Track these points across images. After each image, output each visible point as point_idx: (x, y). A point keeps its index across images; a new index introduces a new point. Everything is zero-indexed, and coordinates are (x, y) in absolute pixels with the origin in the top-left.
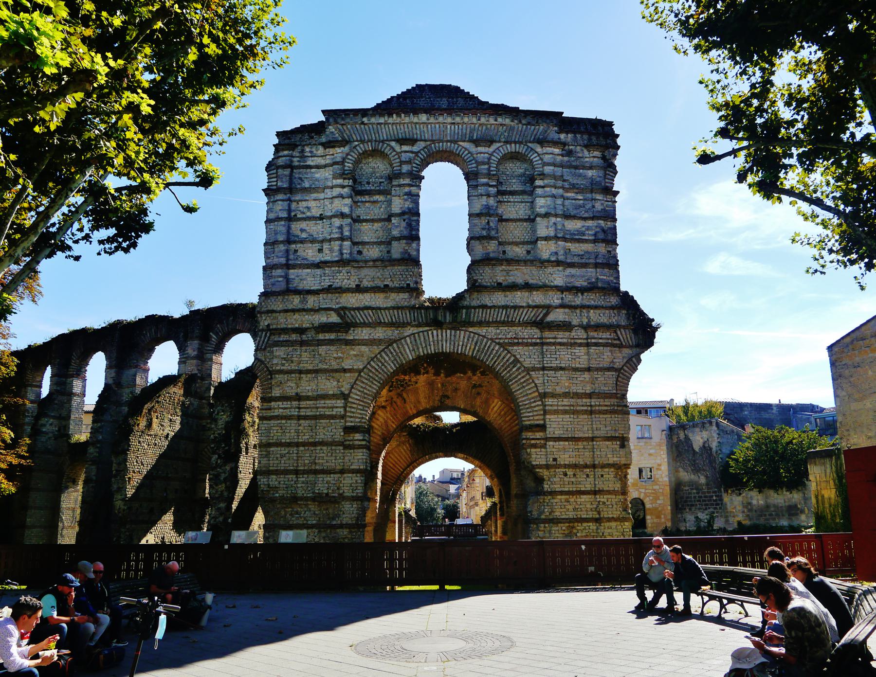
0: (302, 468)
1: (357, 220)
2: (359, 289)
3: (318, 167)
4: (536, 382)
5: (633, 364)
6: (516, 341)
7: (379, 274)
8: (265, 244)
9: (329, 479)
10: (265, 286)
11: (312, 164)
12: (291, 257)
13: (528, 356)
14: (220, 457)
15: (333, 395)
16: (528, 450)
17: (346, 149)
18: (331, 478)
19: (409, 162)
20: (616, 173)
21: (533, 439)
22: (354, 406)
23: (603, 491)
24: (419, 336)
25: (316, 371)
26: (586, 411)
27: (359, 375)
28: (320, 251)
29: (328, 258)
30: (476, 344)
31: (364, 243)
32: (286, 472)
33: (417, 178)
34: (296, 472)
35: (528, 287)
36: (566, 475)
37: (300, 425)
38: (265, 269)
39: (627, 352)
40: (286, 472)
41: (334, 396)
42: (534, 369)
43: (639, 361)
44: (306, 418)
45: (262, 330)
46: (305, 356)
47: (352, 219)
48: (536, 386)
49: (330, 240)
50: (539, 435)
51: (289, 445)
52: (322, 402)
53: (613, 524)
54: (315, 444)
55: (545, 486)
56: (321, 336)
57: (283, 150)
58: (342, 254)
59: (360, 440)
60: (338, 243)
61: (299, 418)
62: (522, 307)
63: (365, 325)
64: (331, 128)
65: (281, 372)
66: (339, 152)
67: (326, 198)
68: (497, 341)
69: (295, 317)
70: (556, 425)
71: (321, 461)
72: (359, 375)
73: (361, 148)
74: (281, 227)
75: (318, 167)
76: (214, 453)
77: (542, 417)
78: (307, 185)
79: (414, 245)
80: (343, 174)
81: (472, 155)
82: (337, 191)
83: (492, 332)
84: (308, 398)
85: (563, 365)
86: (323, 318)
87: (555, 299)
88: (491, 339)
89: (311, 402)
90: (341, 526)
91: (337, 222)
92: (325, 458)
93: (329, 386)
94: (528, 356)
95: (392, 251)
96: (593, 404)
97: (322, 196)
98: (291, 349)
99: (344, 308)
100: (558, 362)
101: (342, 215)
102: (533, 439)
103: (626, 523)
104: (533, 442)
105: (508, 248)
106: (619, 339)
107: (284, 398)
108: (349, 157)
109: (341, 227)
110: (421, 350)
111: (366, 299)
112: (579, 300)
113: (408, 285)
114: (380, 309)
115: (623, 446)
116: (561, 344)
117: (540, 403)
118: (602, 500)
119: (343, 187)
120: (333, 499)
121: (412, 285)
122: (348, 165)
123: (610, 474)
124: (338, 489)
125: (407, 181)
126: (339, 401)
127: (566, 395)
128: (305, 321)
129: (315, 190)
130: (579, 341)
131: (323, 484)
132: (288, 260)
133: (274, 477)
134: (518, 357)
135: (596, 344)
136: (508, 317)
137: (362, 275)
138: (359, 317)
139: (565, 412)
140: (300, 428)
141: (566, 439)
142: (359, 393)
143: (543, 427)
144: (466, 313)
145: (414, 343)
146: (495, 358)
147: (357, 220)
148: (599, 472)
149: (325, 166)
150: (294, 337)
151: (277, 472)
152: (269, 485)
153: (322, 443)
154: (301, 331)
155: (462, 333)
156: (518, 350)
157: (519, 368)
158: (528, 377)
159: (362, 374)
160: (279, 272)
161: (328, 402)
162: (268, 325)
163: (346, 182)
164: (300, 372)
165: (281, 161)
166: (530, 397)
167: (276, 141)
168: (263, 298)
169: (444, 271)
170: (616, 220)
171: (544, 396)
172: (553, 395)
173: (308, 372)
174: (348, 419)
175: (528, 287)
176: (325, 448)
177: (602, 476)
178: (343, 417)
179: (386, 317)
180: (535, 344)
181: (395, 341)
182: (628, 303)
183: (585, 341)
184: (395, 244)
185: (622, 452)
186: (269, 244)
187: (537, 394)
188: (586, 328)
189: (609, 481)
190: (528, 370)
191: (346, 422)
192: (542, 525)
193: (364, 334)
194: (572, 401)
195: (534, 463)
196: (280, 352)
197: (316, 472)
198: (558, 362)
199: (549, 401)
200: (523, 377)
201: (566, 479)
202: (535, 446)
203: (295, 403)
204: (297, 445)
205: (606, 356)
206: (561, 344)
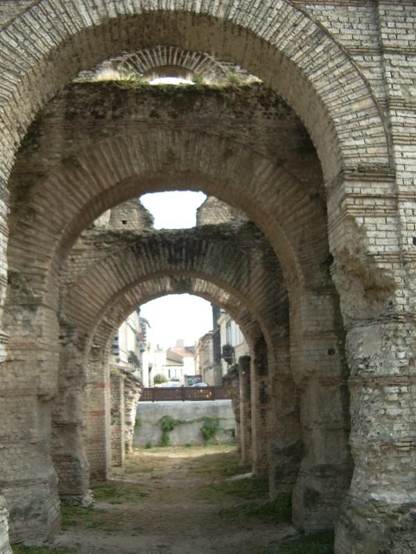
4: (367, 75)
16: (360, 220)
21: (369, 197)
48: (368, 85)
50: (378, 188)
55: (400, 300)
104: (367, 202)
134: (325, 24)
143: (387, 173)
166: (356, 107)
190: (347, 54)
192: (394, 390)
195: (372, 250)
200: (338, 66)
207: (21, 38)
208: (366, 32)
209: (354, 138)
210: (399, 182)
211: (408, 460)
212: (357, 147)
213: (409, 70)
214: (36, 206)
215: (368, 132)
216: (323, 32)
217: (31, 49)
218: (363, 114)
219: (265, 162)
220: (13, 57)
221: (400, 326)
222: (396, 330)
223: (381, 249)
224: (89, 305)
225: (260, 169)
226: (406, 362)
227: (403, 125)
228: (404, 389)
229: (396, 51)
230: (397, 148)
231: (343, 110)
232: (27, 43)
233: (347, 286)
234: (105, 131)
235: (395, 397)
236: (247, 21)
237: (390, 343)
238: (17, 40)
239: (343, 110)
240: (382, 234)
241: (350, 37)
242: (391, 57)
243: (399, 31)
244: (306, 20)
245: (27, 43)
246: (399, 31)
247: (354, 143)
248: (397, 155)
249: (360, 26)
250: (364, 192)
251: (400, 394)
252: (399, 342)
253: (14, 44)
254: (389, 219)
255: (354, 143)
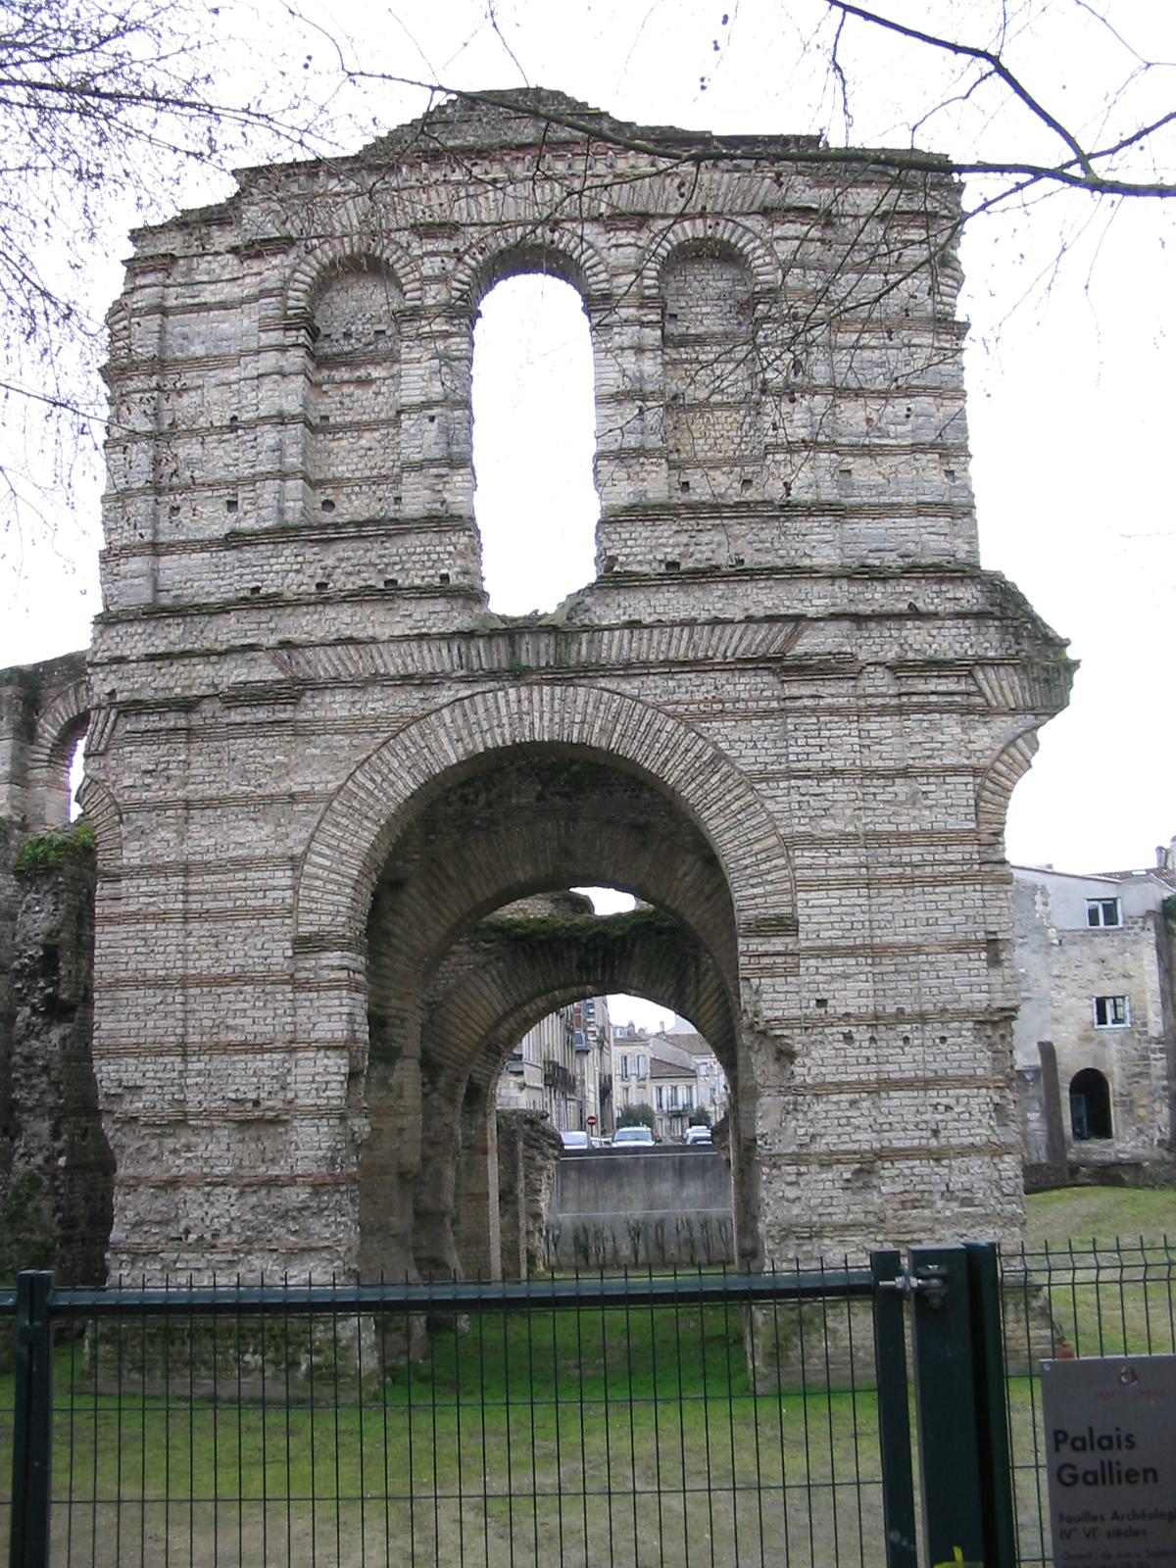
0: (196, 1039)
1: (319, 427)
2: (323, 596)
3: (223, 305)
4: (770, 805)
5: (1017, 754)
6: (717, 707)
7: (372, 556)
8: (104, 499)
9: (261, 1065)
10: (107, 598)
11: (212, 299)
12: (164, 524)
13: (747, 745)
14: (35, 1011)
15: (267, 858)
17: (290, 259)
18: (263, 1063)
19: (443, 278)
20: (960, 282)
21: (766, 954)
22: (318, 883)
23: (946, 1078)
24: (473, 705)
25: (221, 802)
26: (901, 876)
27: (329, 808)
28: (232, 505)
29: (249, 524)
30: (616, 718)
31: (338, 483)
32: (160, 1051)
33: (464, 312)
34: (184, 1050)
35: (743, 573)
36: (848, 1038)
37: (189, 935)
38: (105, 557)
39: (1005, 726)
40: (160, 1051)
41: (268, 861)
42: (766, 777)
43: (1034, 746)
44: (205, 916)
45: (99, 707)
46: (200, 765)
47: (307, 424)
49: (253, 480)
50: (778, 944)
51: (161, 984)
52: (241, 875)
53: (975, 1163)
54: (221, 981)
56: (235, 717)
57: (144, 273)
58: (281, 512)
59: (333, 968)
60: (273, 485)
61: (186, 917)
62: (731, 622)
63: (336, 683)
64: (251, 213)
65: (142, 806)
66: (272, 270)
67: (243, 374)
68: (669, 708)
69: (173, 669)
70: (823, 914)
71: (238, 1021)
72: (329, 808)
73: (326, 253)
74: (141, 456)
75: (223, 305)
76: (23, 1001)
77: (786, 898)
78: (198, 350)
79: (458, 478)
80: (285, 317)
81: (597, 253)
82: (269, 361)
83: (653, 688)
84: (207, 868)
85: (839, 764)
86: (235, 673)
87: (815, 599)
88: (658, 708)
89: (213, 878)
90: (292, 1181)
91: (269, 436)
92: (253, 1015)
93: (253, 836)
94: (747, 745)
95: (406, 497)
96: (916, 858)
97: (232, 375)
98: (164, 749)
99: (286, 645)
100: (826, 756)
101: (281, 419)
102: (766, 954)
103: (1006, 1158)
104: (765, 961)
105: (694, 477)
106: (981, 693)
107: (158, 870)
108: (297, 275)
109: (279, 448)
110: (478, 738)
111: (343, 620)
112: (878, 597)
113: (445, 578)
114: (374, 640)
115: (995, 962)
116: (832, 711)
117: (782, 861)
118: (945, 1101)
119: (283, 349)
120: (270, 1114)
121: (453, 580)
122: (297, 299)
123: (964, 1036)
124: (283, 1088)
125: (439, 325)
126: (280, 874)
127: (846, 839)
128: (201, 676)
129: (220, 361)
130: (879, 701)
131: (246, 1077)
132: (156, 533)
133: (132, 1061)
134: (723, 746)
135: (922, 708)
136: (695, 648)
137: (330, 562)
138: (324, 664)
139: (848, 883)
140: (191, 940)
141: (851, 952)
142: (328, 852)
143: (786, 925)
144: (590, 642)
145: (460, 721)
146: (664, 753)
147: (319, 427)
148: (934, 1031)
149: (243, 301)
150: (173, 720)
151: (137, 1051)
152: (120, 1080)
153: (240, 978)
154: (187, 705)
155: (581, 691)
156: (723, 731)
157: (728, 775)
158: (749, 798)
159: (335, 804)
160: (137, 564)
161: (251, 875)
162: (112, 694)
163: (292, 337)
164: (188, 805)
165: (141, 299)
166: (757, 847)
167: (129, 251)
168: (100, 627)
169: (537, 542)
170: (964, 394)
171: (789, 843)
172: (813, 841)
173: (207, 803)
174: (303, 918)
175: (743, 573)
176: (249, 989)
177: (943, 1039)
178: (291, 911)
179: (393, 662)
180: (767, 713)
181: (416, 720)
182: (1004, 606)
183: (895, 701)
184: (409, 479)
185: (996, 977)
186: (117, 499)
187: (774, 840)
188: (898, 668)
189: (965, 1052)
191: (298, 924)
193: (337, 706)
194: (862, 855)
196: (142, 757)
197: (226, 1048)
198: (826, 756)
199: (803, 857)
200: (738, 798)
201: (851, 1051)
202: (769, 971)
203: (176, 881)
204: (184, 982)
205: (952, 738)
206: (832, 711)
207: (379, 779)
208: (773, 751)
209: (753, 886)
210: (801, 936)
211: (809, 1248)
212: (755, 897)
213: (821, 798)
214: (390, 926)
215: (769, 878)
216: (719, 757)
217: (391, 791)
218: (764, 855)
219: (690, 858)
220: (371, 801)
221: (800, 1099)
222: (795, 1103)
223: (779, 1014)
224: (462, 1036)
225: (685, 868)
226: (807, 1139)
227: (810, 867)
228: (803, 1169)
229: (807, 775)
230: (801, 895)
231: (741, 852)
232: (385, 785)
233: (756, 1047)
234: (477, 823)
235: (793, 1178)
236: (629, 749)
237: (789, 1117)
238: (373, 781)
239: (741, 852)
240: (781, 996)
241: (753, 760)
242: (799, 783)
243: (812, 750)
244: (701, 743)
245: (385, 785)
246: (812, 750)
247: (752, 891)
248: (799, 904)
249: (766, 745)
250: (761, 949)
251: (799, 1174)
252: (800, 1116)
253: (371, 786)
254: (789, 979)
255: (752, 891)
